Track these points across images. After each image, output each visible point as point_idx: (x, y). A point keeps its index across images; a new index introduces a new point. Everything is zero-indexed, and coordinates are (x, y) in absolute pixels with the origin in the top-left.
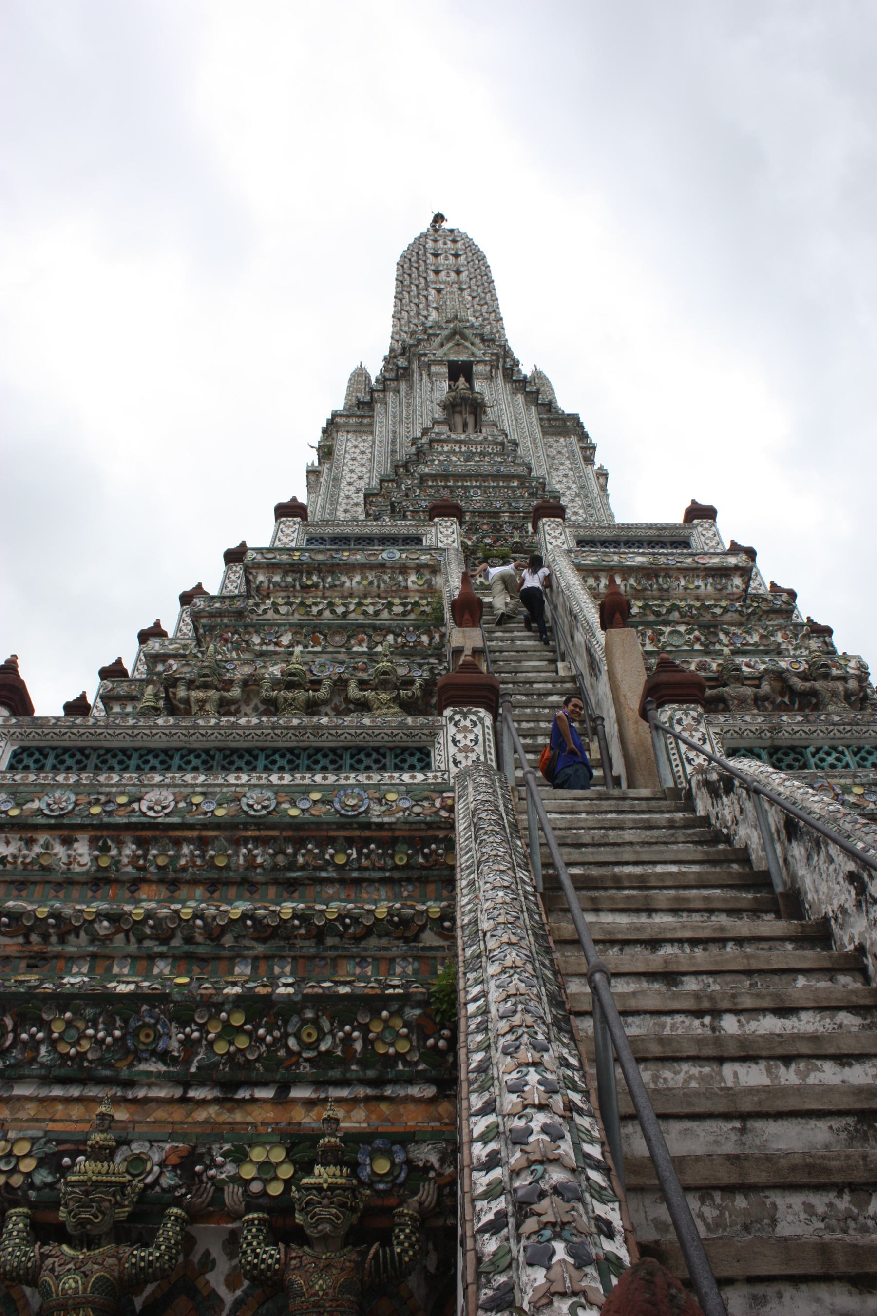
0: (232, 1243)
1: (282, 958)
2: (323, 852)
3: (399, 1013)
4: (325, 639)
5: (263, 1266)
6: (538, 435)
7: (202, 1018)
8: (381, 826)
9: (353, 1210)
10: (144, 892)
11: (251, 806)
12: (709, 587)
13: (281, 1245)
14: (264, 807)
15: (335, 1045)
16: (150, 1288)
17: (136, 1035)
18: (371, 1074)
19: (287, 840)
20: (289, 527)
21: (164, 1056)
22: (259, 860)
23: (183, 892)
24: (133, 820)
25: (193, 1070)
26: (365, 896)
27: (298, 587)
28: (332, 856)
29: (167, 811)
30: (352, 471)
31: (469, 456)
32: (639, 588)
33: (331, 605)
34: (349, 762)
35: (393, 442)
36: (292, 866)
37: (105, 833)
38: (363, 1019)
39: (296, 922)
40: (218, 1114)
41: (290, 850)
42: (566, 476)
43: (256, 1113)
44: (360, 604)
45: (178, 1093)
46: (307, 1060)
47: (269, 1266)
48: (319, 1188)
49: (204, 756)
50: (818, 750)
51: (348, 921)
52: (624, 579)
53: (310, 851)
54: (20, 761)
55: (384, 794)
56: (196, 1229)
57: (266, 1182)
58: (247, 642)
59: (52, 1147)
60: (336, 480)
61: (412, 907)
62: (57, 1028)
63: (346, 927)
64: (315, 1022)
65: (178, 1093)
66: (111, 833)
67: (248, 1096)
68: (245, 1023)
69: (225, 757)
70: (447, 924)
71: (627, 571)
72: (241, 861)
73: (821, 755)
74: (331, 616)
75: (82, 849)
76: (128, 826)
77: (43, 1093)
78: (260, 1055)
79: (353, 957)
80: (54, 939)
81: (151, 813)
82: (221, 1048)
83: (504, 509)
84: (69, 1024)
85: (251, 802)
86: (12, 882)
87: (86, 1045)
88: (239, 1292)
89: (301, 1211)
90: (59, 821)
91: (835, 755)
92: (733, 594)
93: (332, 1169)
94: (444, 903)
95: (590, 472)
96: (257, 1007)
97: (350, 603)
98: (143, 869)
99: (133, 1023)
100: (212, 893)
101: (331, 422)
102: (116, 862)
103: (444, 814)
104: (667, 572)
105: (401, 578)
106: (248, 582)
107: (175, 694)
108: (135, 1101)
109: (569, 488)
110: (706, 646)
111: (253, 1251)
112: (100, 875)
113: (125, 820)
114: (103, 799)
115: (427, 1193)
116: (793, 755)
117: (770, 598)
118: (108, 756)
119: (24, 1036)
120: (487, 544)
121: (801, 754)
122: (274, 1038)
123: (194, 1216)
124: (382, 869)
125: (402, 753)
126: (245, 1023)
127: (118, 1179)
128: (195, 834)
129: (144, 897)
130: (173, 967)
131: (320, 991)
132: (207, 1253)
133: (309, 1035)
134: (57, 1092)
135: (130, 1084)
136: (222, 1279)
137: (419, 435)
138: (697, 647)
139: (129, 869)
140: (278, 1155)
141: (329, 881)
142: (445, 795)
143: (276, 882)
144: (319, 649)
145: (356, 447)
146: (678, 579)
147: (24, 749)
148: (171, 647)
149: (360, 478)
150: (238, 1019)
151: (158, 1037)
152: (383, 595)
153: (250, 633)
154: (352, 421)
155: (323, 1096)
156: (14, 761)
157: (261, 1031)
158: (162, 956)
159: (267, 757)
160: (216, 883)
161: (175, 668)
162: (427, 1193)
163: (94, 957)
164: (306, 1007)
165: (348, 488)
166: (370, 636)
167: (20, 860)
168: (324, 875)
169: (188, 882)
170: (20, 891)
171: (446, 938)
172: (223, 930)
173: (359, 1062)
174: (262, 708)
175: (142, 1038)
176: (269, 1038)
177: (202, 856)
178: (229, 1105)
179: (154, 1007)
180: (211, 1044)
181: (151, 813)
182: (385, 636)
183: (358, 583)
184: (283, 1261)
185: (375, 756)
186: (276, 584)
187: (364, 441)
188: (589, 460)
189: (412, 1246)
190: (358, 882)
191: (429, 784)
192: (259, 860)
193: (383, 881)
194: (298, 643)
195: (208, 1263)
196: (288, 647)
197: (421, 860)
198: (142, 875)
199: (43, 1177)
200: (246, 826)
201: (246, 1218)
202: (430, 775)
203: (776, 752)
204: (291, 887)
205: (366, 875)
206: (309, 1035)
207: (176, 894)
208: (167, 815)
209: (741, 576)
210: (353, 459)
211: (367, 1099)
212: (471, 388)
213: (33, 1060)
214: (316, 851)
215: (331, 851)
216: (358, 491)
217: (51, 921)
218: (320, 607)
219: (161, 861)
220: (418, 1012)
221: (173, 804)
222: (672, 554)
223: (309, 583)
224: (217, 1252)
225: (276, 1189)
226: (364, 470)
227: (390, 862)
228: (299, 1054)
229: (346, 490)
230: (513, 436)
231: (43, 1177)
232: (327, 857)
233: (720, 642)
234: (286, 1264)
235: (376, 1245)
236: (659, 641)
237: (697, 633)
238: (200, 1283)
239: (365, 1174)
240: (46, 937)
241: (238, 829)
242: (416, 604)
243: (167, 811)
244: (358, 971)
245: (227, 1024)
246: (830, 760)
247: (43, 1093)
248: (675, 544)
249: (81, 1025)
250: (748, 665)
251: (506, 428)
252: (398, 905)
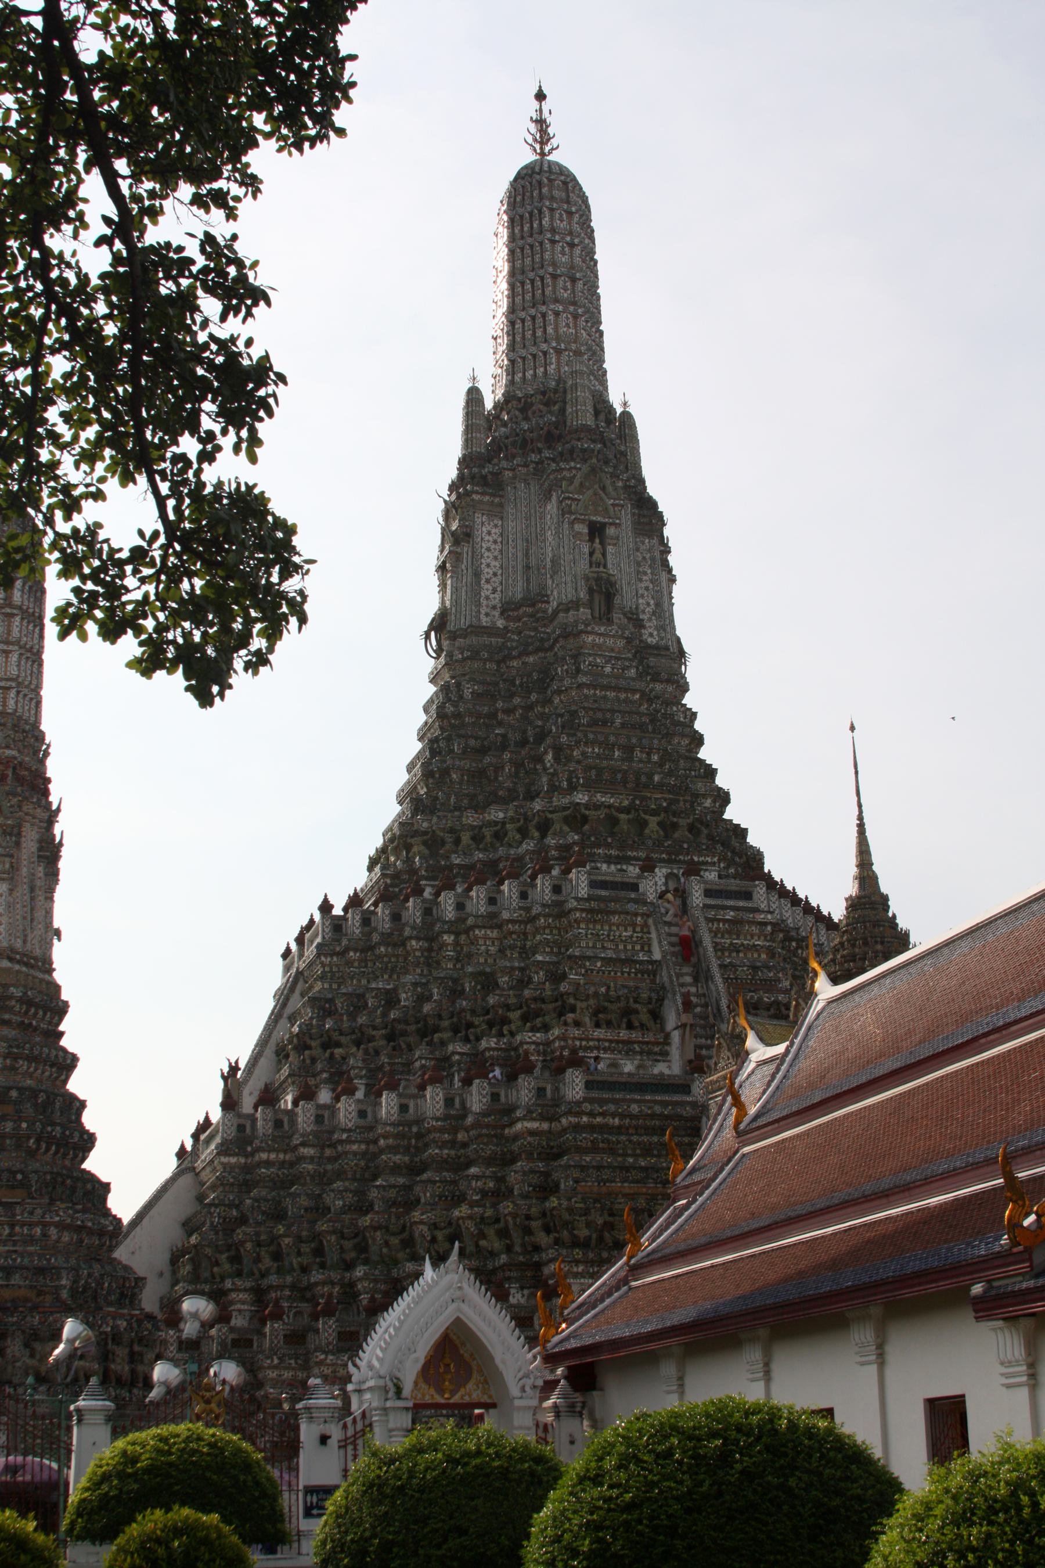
30: (488, 565)
60: (477, 574)
75: (617, 1120)
109: (648, 604)
145: (489, 533)
187: (496, 526)
216: (494, 591)
229: (486, 589)
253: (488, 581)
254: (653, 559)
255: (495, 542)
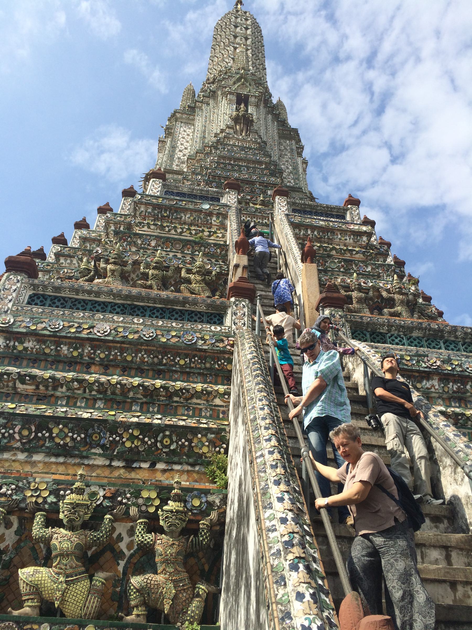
0: (131, 532)
1: (154, 404)
2: (174, 360)
3: (206, 435)
4: (172, 245)
5: (145, 542)
6: (276, 138)
7: (120, 431)
8: (201, 350)
9: (184, 521)
10: (93, 369)
11: (144, 335)
12: (351, 240)
13: (153, 533)
14: (150, 336)
15: (177, 448)
16: (94, 548)
17: (91, 436)
18: (191, 460)
19: (159, 352)
20: (157, 184)
21: (103, 447)
22: (146, 360)
23: (111, 370)
24: (90, 336)
25: (115, 453)
26: (191, 379)
27: (160, 216)
28: (178, 361)
29: (106, 334)
30: (182, 144)
31: (243, 148)
32: (319, 237)
33: (175, 228)
34: (187, 317)
35: (205, 132)
36: (160, 363)
37: (77, 341)
38: (189, 437)
39: (162, 390)
40: (124, 473)
41: (160, 357)
42: (287, 161)
43: (140, 474)
44: (189, 229)
45: (107, 463)
46: (164, 452)
47: (148, 542)
48: (172, 511)
49: (122, 307)
50: (392, 335)
51: (184, 391)
52: (313, 232)
53: (169, 358)
54: (33, 301)
55: (201, 334)
56: (115, 525)
57: (147, 506)
58: (134, 242)
59: (55, 487)
60: (173, 147)
61: (211, 387)
62: (55, 431)
63: (183, 394)
64: (170, 437)
65: (107, 463)
66: (79, 341)
67: (138, 466)
68: (139, 435)
69: (132, 309)
70: (226, 397)
71: (313, 228)
72: (138, 359)
73: (393, 338)
74: (174, 233)
76: (88, 339)
77: (47, 460)
78: (145, 448)
79: (184, 406)
80: (50, 388)
81: (99, 334)
82: (128, 444)
83: (257, 180)
84: (61, 430)
85: (144, 333)
86: (30, 359)
87: (68, 440)
88: (132, 551)
89: (163, 520)
90: (55, 334)
91: (399, 339)
92: (361, 245)
93: (177, 503)
94: (226, 387)
95: (299, 160)
96: (146, 429)
97: (184, 228)
98: (93, 359)
99: (90, 431)
100: (124, 372)
101: (174, 115)
102: (81, 355)
103: (229, 347)
104: (332, 231)
105: (209, 218)
106: (135, 210)
107: (99, 265)
108: (88, 465)
109: (288, 168)
110: (346, 270)
111: (142, 535)
112: (72, 360)
113: (87, 336)
114: (76, 325)
115: (214, 515)
116: (380, 337)
117: (379, 247)
118: (77, 302)
119: (40, 435)
120: (247, 199)
121: (384, 336)
122: (152, 442)
123: (116, 519)
124: (200, 369)
125: (211, 316)
126: (139, 435)
127: (85, 503)
128: (119, 345)
129: (93, 371)
130: (105, 404)
131: (172, 423)
132: (120, 534)
133: (167, 442)
134: (53, 459)
135: (87, 457)
136: (125, 546)
137: (218, 132)
138: (342, 270)
139: (87, 358)
140: (154, 495)
141: (176, 372)
142: (229, 339)
143: (153, 370)
144: (169, 250)
145: (185, 131)
146: (337, 235)
147: (35, 295)
148: (93, 235)
149: (186, 149)
150: (136, 433)
151: (101, 438)
152: (200, 225)
153: (136, 238)
154: (184, 116)
155: (170, 468)
156: (30, 300)
157: (146, 439)
158: (100, 399)
159: (151, 311)
160: (126, 369)
161: (100, 252)
162: (214, 515)
163: (68, 397)
164: (166, 430)
165: (179, 153)
166: (193, 247)
167: (35, 350)
168: (174, 368)
169: (113, 366)
170: (34, 364)
171: (225, 402)
172: (129, 390)
173: (186, 455)
174: (140, 276)
175: (94, 438)
176: (149, 442)
177: (121, 355)
178: (129, 470)
179: (100, 425)
180: (124, 443)
181: (99, 334)
182: (200, 247)
183: (189, 218)
184: (154, 540)
185: (199, 315)
186: (149, 213)
187: (190, 128)
188: (300, 154)
189: (206, 538)
190: (188, 373)
191: (222, 332)
192: (146, 360)
193: (199, 374)
194: (159, 246)
195: (120, 538)
196: (154, 247)
197: (217, 366)
198: (92, 361)
199: (52, 499)
200: (142, 344)
201: (139, 521)
202: (223, 328)
203: (373, 334)
204: (159, 374)
205: (192, 371)
206: (167, 442)
207: (107, 371)
208: (106, 336)
209: (367, 236)
210: (183, 138)
211: (188, 471)
212: (247, 111)
213: (43, 445)
214: (172, 358)
215: (178, 359)
216: (184, 155)
217: (50, 380)
218: (170, 228)
219: (102, 356)
220: (213, 436)
221: (109, 331)
222: (337, 222)
223: (165, 215)
224: (124, 535)
225: (152, 510)
226: (188, 144)
227: (203, 366)
228: (162, 450)
230: (265, 139)
231: (52, 499)
232: (176, 361)
233: (353, 269)
234: (155, 542)
235: (192, 536)
236: (325, 265)
237: (343, 263)
238: (116, 547)
239: (189, 506)
240: (47, 387)
241: (138, 345)
242: (215, 232)
243: (106, 334)
244: (186, 412)
245: (132, 434)
246: (397, 341)
247: (47, 460)
248: (338, 217)
249: (66, 430)
250: (364, 283)
251: (262, 134)
252: (206, 386)
253: (180, 151)
254: (292, 150)
255: (188, 135)
